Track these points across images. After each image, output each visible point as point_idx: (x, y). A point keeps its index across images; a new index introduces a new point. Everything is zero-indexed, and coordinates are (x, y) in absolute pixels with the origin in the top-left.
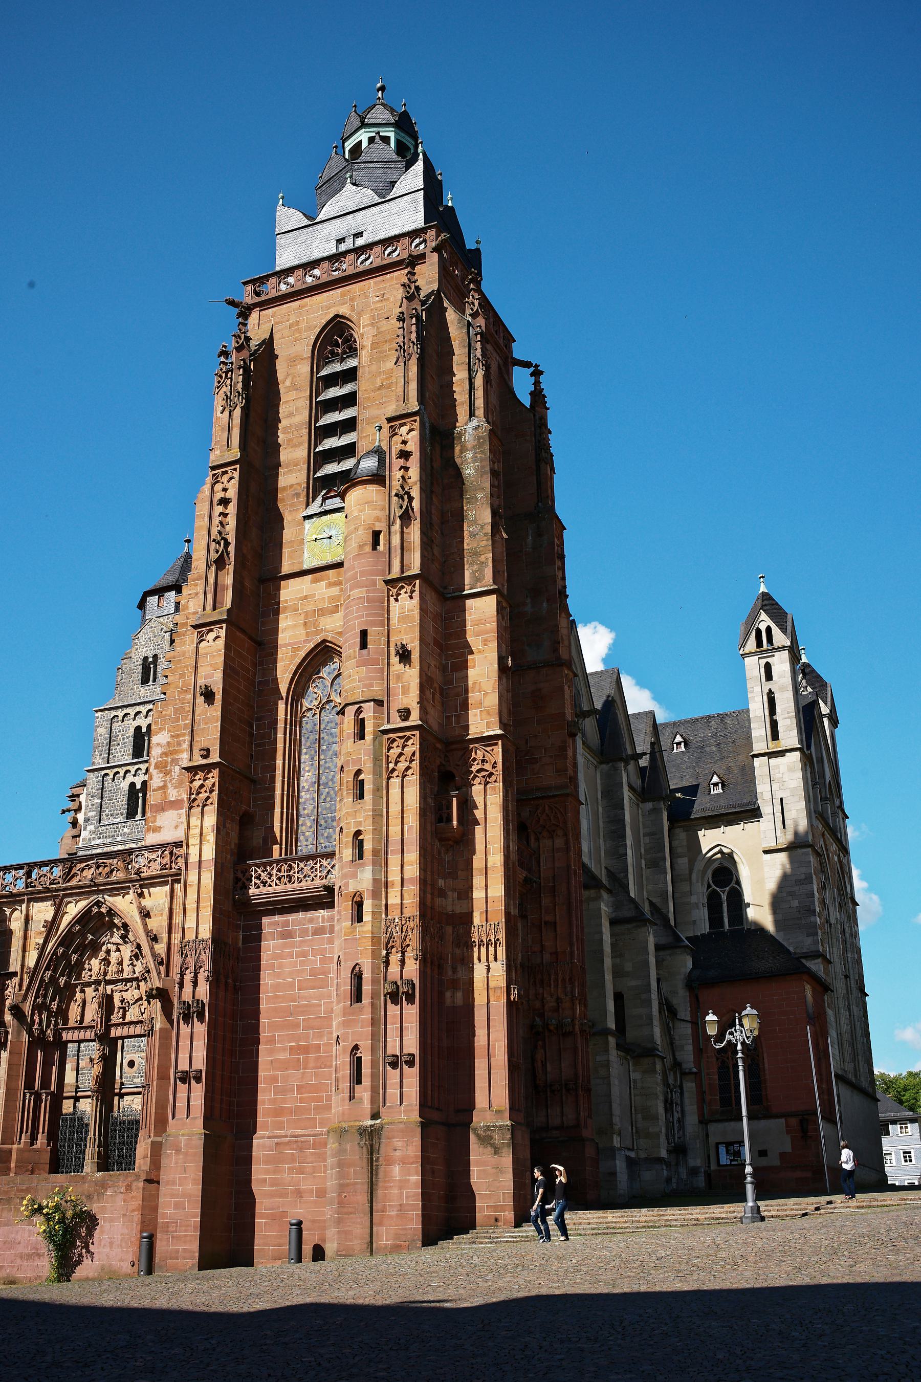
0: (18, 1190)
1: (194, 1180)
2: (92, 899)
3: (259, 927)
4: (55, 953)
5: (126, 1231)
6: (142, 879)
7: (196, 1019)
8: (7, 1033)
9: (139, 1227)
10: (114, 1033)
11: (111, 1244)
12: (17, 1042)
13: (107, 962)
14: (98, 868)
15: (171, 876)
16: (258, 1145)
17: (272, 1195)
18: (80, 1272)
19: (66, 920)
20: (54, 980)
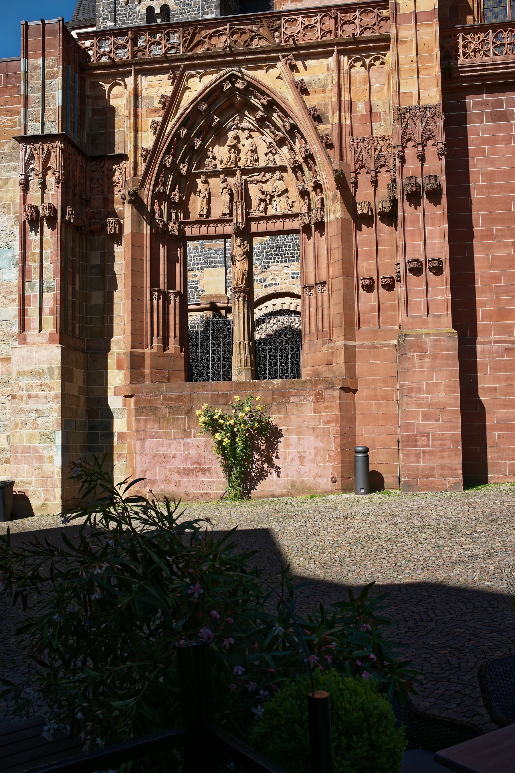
0: (165, 399)
1: (447, 386)
2: (221, 73)
3: (464, 107)
4: (177, 134)
5: (321, 445)
6: (297, 48)
7: (426, 201)
8: (121, 226)
9: (338, 440)
10: (254, 228)
11: (302, 458)
12: (136, 235)
13: (235, 148)
14: (232, 34)
15: (338, 44)
16: (483, 351)
17: (505, 405)
18: (262, 488)
19: (187, 98)
20: (174, 167)
